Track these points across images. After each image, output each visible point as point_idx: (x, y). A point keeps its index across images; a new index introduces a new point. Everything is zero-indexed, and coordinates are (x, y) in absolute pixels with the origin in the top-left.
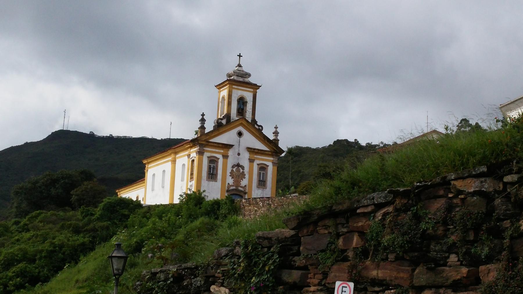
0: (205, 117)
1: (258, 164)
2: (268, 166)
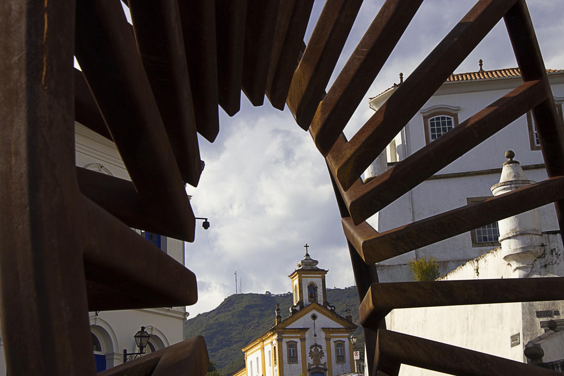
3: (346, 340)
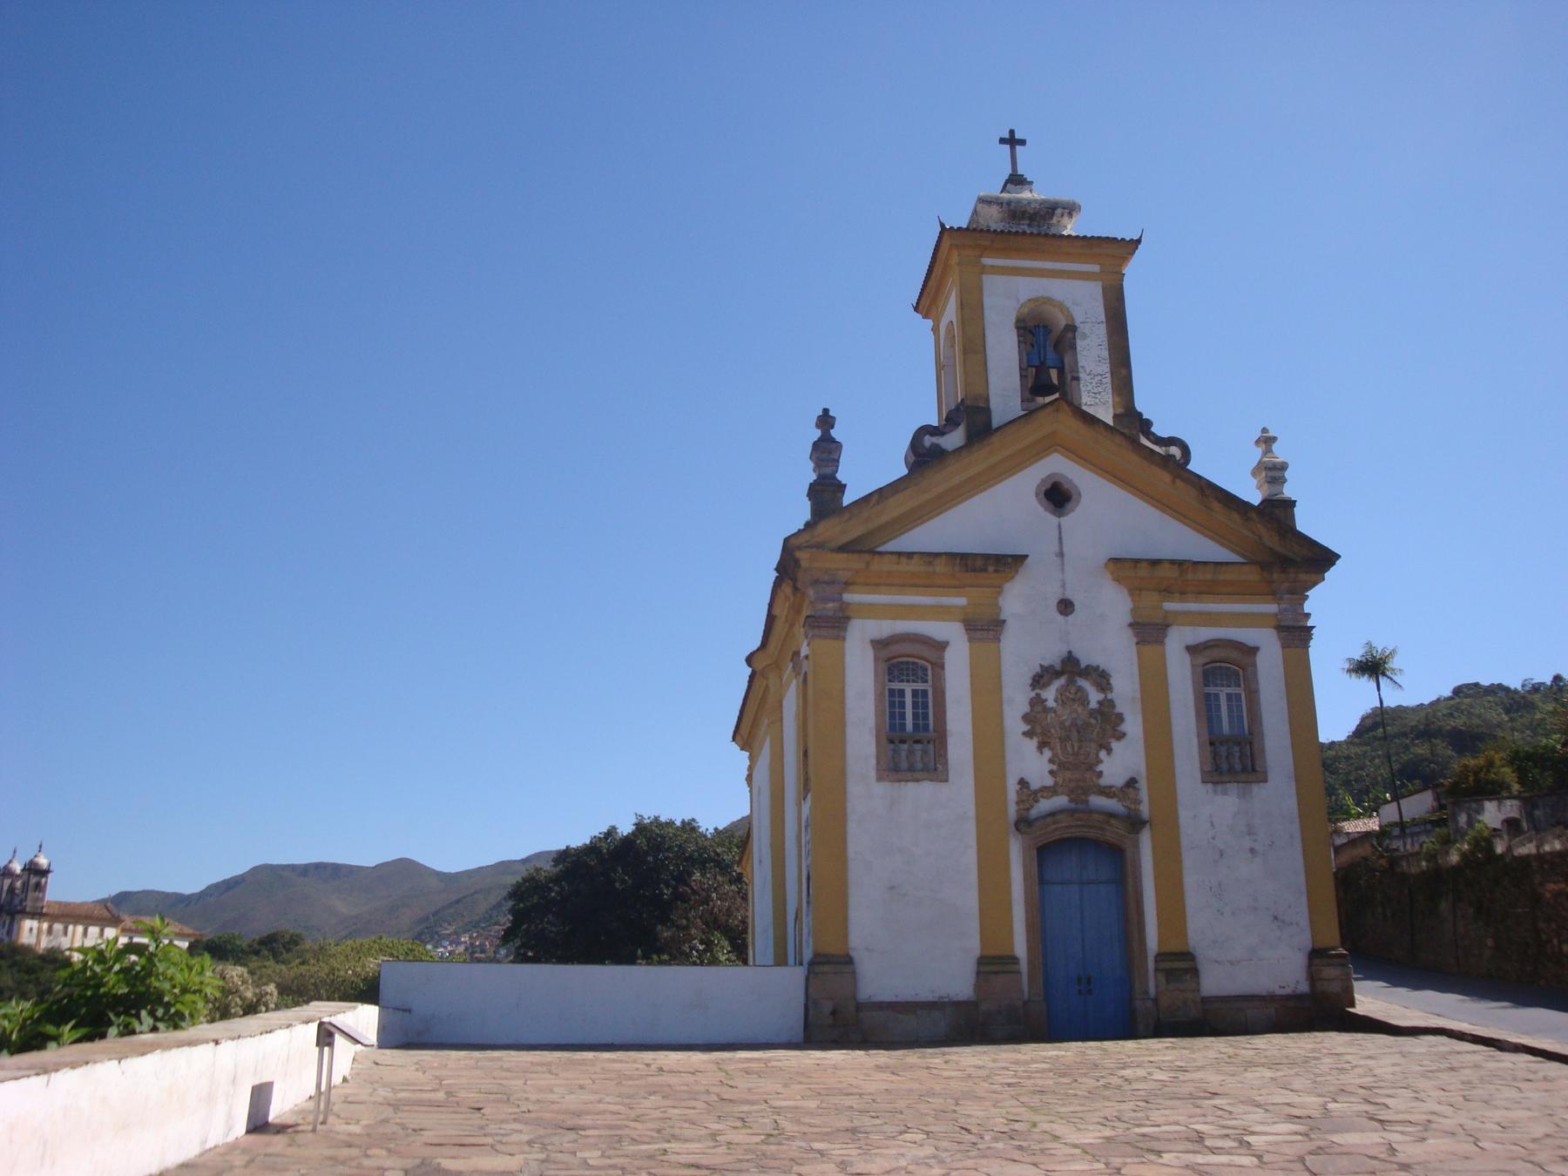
0: (835, 433)
1: (1192, 650)
2: (1254, 651)
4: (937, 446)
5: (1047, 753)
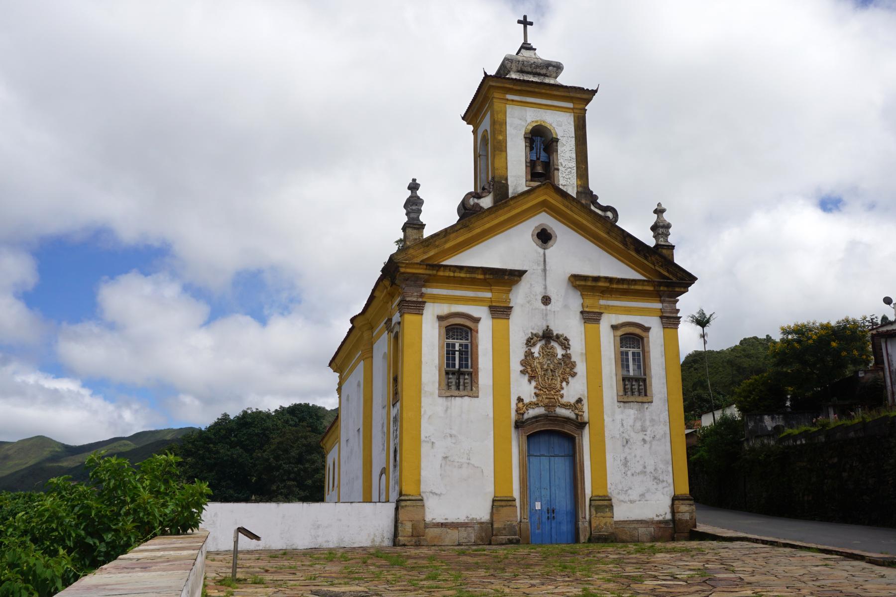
1: (614, 328)
2: (647, 329)
3: (654, 323)
4: (478, 204)
5: (534, 383)
